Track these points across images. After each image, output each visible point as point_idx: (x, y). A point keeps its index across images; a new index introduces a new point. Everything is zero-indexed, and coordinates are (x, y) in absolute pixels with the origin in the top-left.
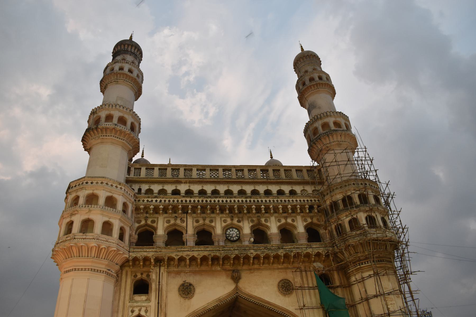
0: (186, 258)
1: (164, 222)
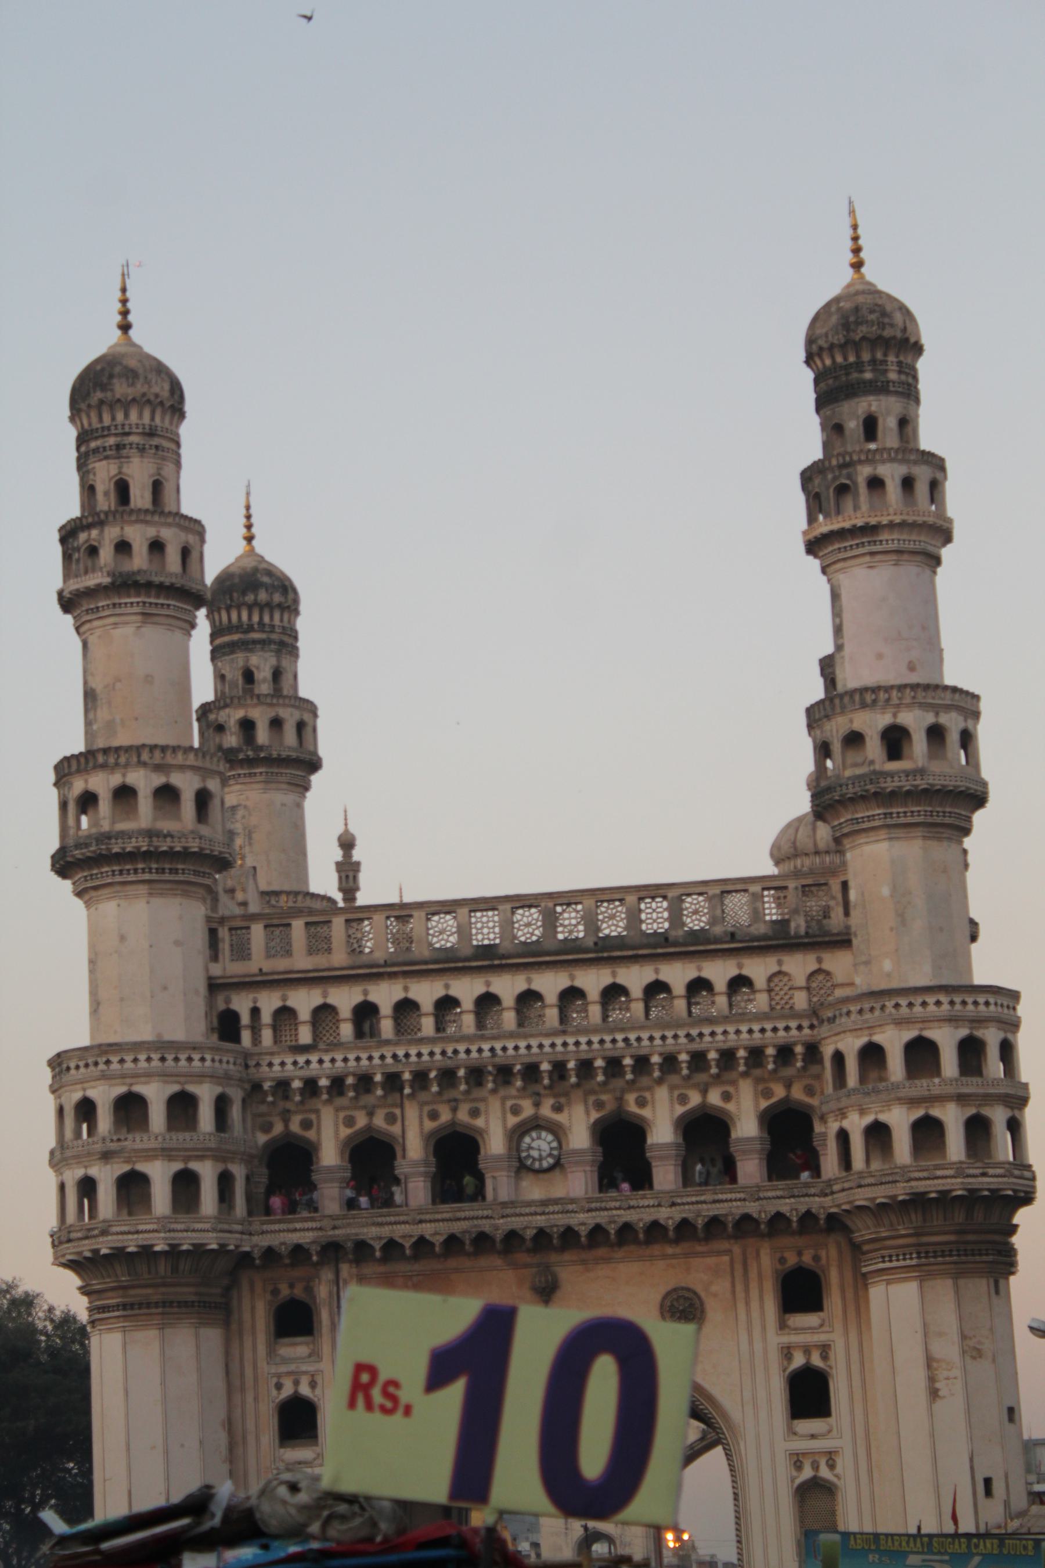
0: (402, 1246)
1: (336, 1125)
